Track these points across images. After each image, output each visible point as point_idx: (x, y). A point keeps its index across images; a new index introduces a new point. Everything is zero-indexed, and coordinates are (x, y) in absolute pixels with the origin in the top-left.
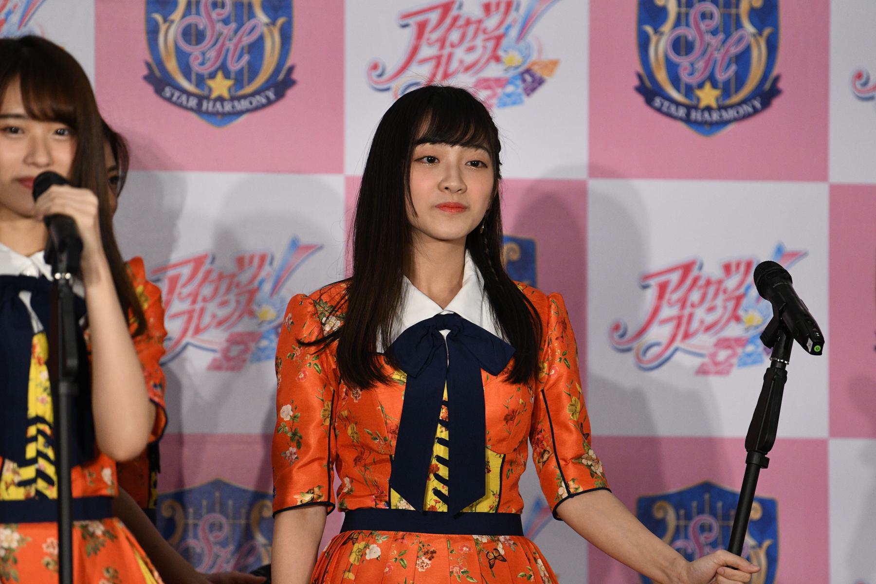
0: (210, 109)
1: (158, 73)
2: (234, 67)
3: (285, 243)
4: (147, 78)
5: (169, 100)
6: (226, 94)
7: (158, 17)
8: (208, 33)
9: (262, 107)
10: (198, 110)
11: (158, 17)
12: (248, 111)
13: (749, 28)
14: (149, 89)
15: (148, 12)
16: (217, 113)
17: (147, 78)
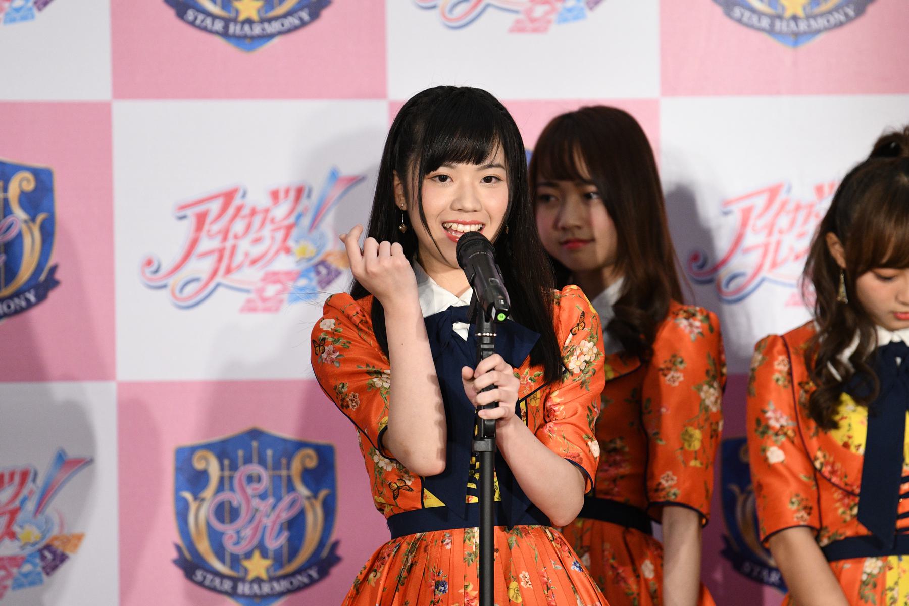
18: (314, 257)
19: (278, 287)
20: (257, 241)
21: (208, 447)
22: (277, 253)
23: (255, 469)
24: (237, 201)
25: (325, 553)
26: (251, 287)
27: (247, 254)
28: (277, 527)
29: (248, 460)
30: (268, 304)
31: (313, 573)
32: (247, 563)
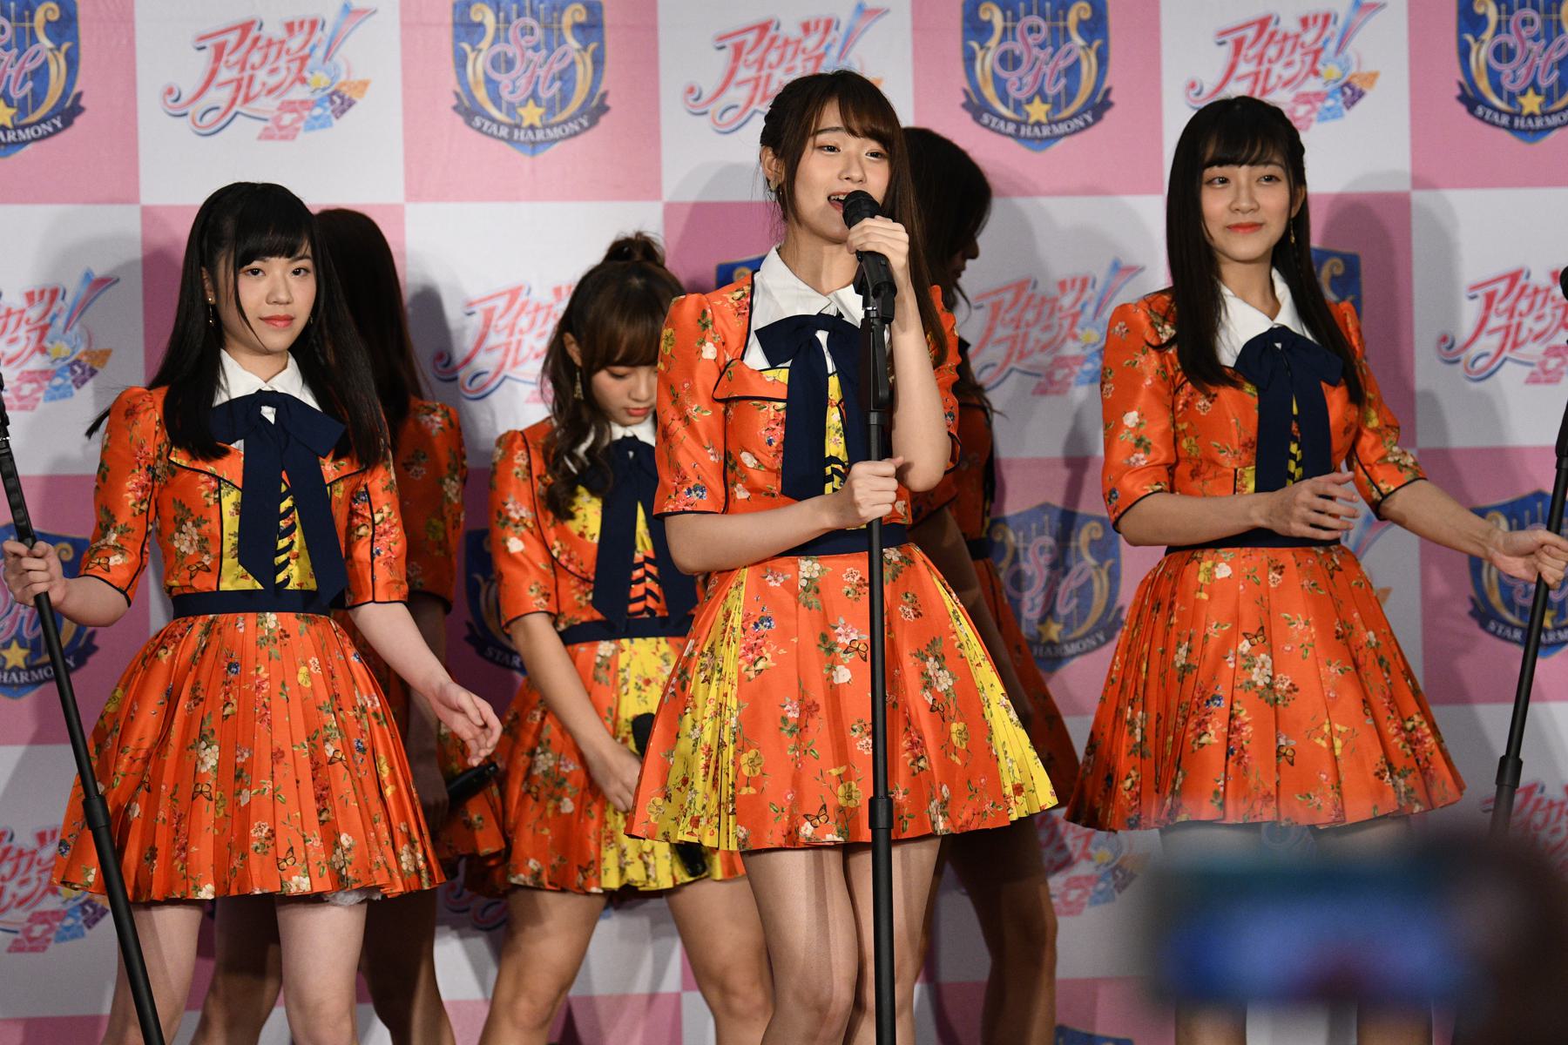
0: (1029, 134)
1: (975, 100)
2: (1051, 91)
3: (1106, 265)
4: (964, 106)
5: (987, 126)
6: (1044, 119)
7: (975, 45)
8: (1025, 58)
9: (1081, 129)
10: (1016, 136)
11: (975, 45)
12: (1066, 134)
13: (1078, 40)
14: (968, 117)
15: (965, 40)
16: (1035, 138)
17: (964, 106)
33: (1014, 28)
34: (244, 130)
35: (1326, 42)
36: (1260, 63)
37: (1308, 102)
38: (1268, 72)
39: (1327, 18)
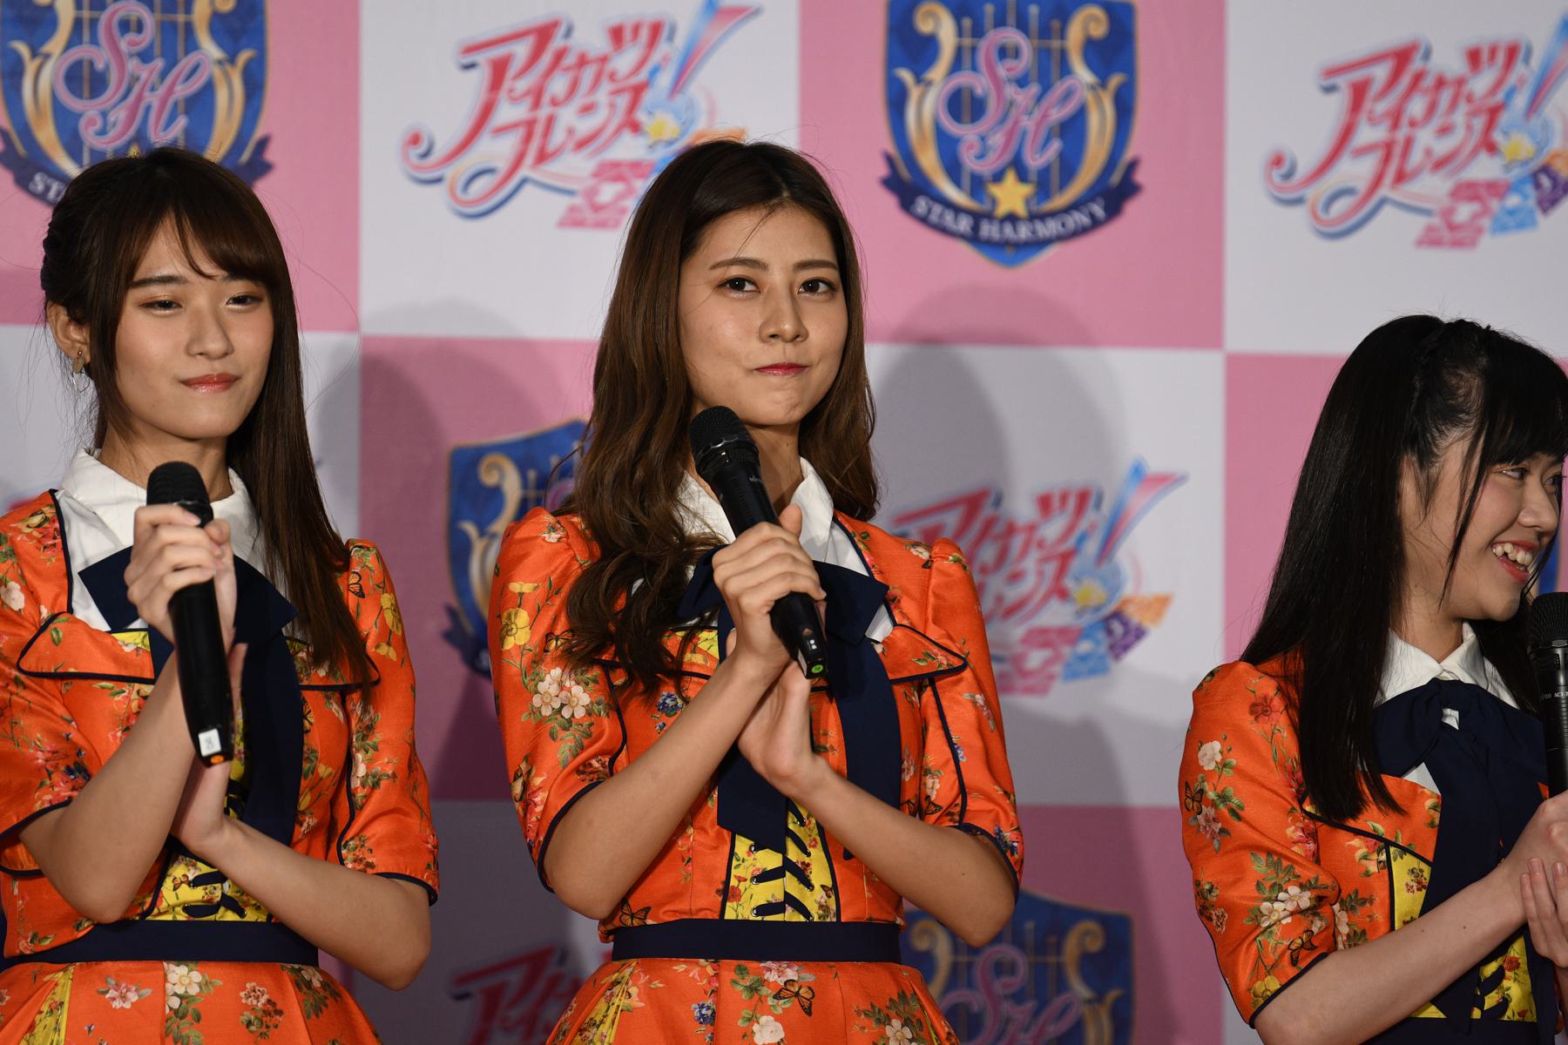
18: (676, 140)
19: (618, 187)
20: (588, 109)
21: (507, 449)
22: (618, 132)
23: (1011, 36)
24: (557, 42)
25: (1116, 178)
26: (573, 187)
27: (571, 131)
28: (1043, 133)
29: (1000, 22)
30: (602, 216)
31: (1098, 210)
32: (995, 190)
33: (94, 23)
34: (1394, 229)
35: (655, 71)
36: (536, 105)
37: (619, 178)
38: (550, 121)
39: (656, 29)
